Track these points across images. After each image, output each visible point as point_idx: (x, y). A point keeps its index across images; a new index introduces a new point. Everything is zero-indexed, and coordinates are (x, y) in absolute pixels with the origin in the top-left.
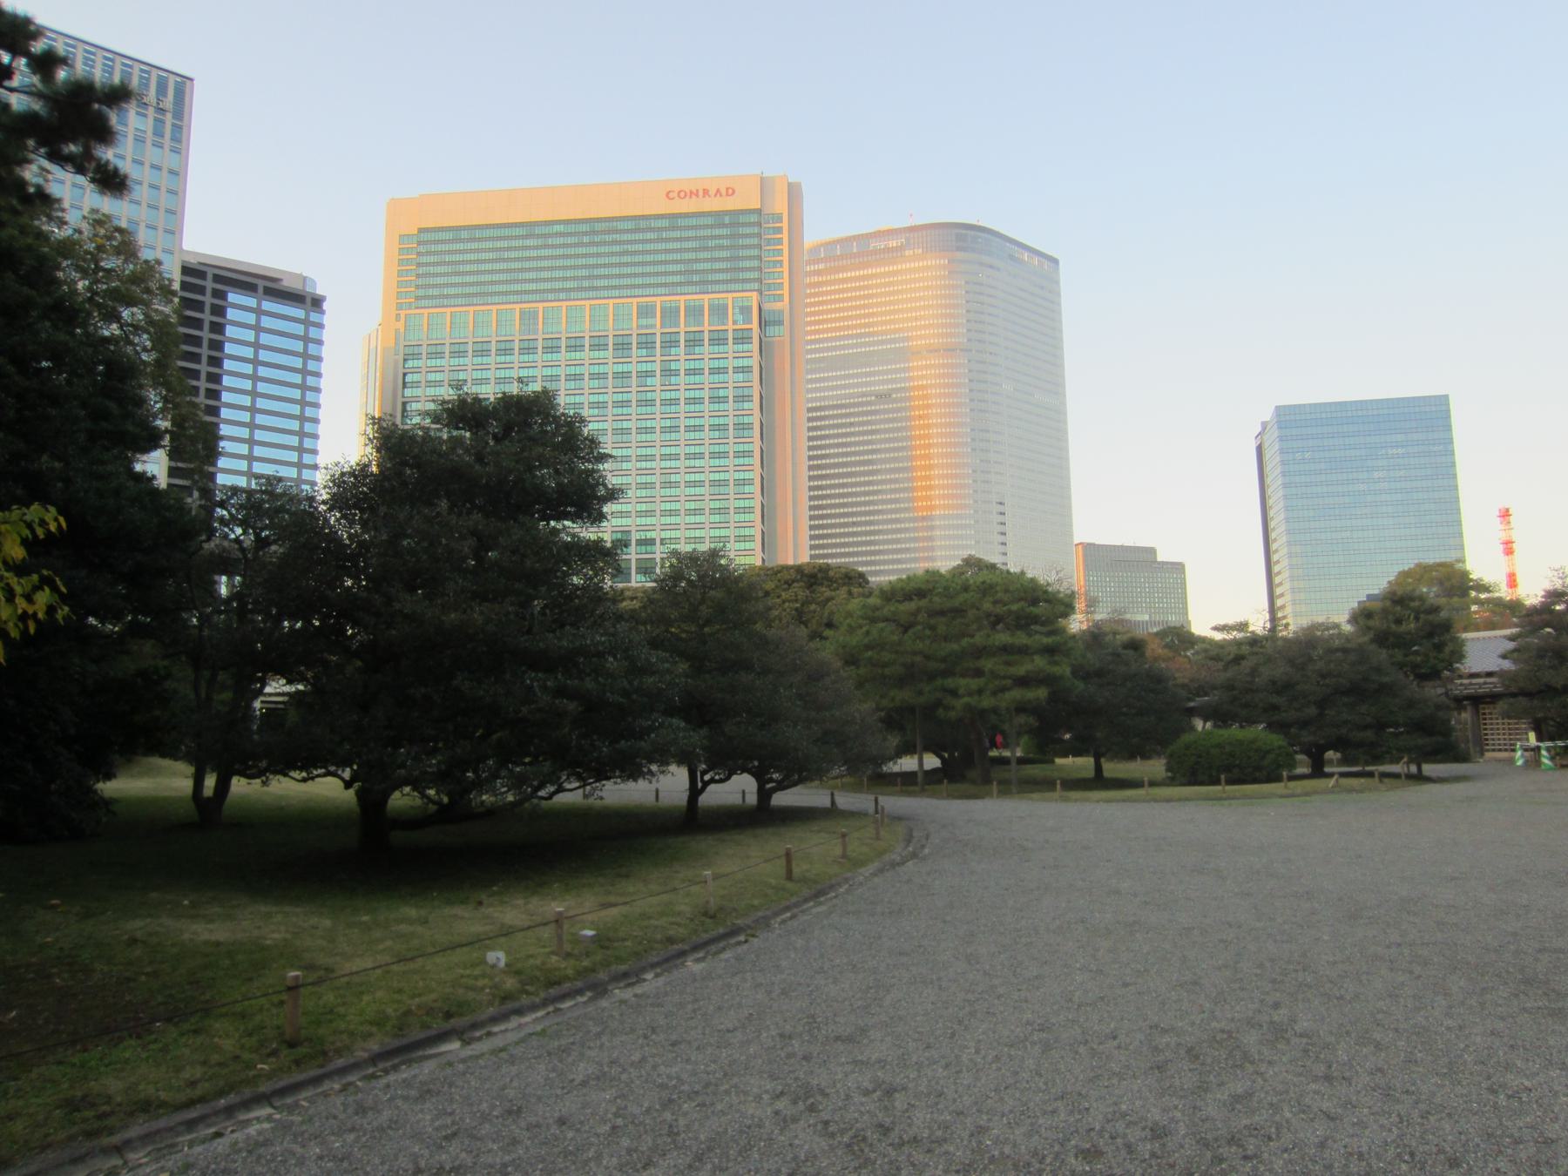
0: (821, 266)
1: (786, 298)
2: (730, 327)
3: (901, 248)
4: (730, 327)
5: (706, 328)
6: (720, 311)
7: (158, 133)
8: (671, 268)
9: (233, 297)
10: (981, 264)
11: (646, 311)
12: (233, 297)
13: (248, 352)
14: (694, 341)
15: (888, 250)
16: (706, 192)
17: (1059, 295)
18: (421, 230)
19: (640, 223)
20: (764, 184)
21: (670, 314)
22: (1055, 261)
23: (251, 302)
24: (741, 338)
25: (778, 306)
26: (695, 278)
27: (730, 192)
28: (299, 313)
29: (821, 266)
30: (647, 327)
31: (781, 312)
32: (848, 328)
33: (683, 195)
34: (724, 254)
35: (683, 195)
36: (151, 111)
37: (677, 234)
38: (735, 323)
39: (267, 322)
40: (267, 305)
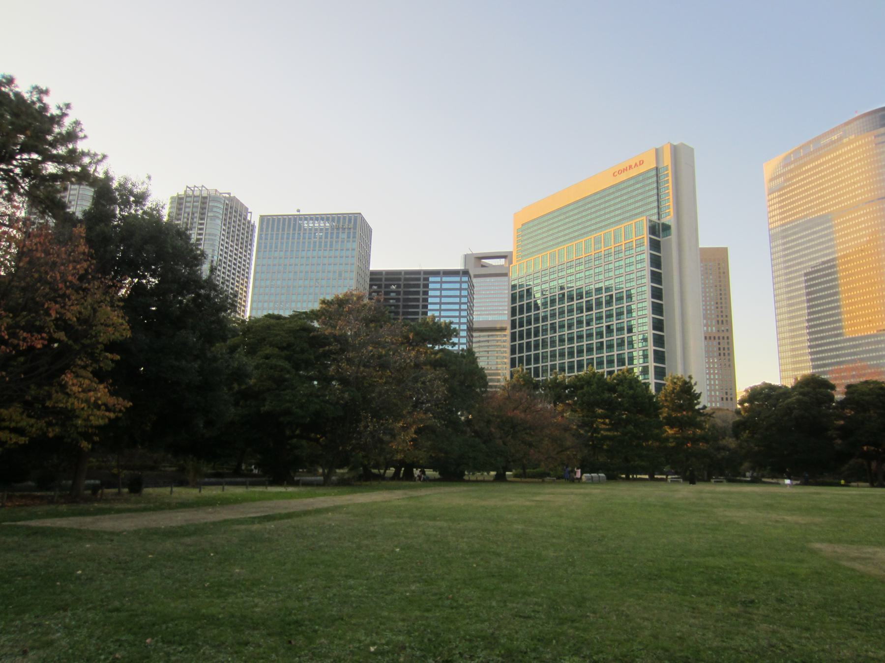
0: (792, 166)
3: (840, 139)
7: (348, 237)
8: (617, 212)
9: (431, 279)
11: (597, 241)
12: (431, 279)
13: (437, 300)
15: (834, 142)
19: (604, 194)
23: (438, 279)
26: (628, 215)
27: (641, 163)
28: (457, 279)
29: (792, 166)
32: (811, 201)
33: (620, 172)
34: (639, 198)
35: (620, 172)
36: (346, 231)
37: (619, 193)
39: (445, 286)
40: (444, 279)
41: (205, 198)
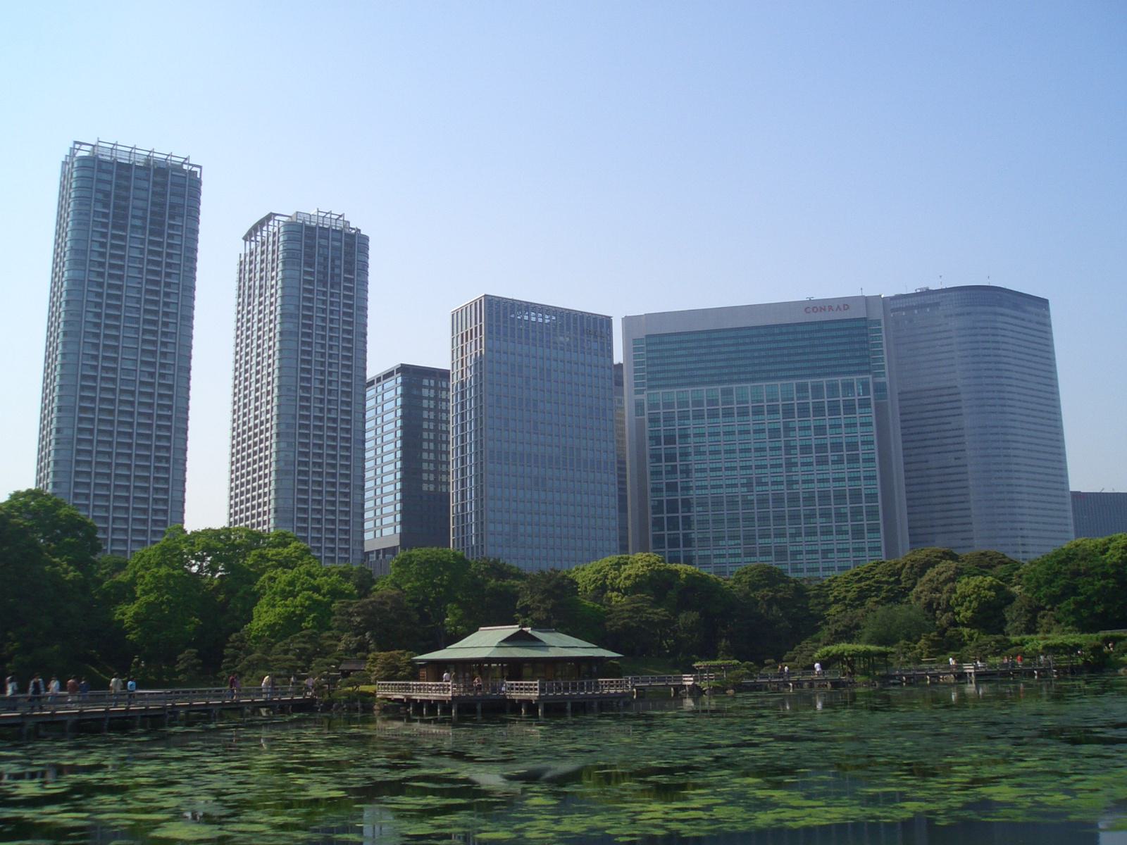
1: (887, 374)
2: (856, 398)
4: (856, 398)
5: (841, 398)
6: (849, 386)
10: (996, 314)
11: (802, 389)
14: (834, 409)
16: (830, 308)
17: (1050, 326)
18: (648, 336)
20: (867, 300)
21: (817, 390)
22: (1044, 303)
24: (865, 404)
25: (882, 380)
30: (803, 398)
31: (884, 383)
38: (859, 395)
41: (353, 236)
